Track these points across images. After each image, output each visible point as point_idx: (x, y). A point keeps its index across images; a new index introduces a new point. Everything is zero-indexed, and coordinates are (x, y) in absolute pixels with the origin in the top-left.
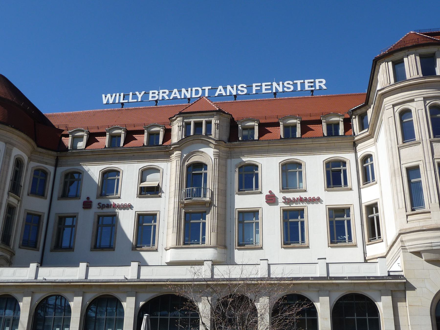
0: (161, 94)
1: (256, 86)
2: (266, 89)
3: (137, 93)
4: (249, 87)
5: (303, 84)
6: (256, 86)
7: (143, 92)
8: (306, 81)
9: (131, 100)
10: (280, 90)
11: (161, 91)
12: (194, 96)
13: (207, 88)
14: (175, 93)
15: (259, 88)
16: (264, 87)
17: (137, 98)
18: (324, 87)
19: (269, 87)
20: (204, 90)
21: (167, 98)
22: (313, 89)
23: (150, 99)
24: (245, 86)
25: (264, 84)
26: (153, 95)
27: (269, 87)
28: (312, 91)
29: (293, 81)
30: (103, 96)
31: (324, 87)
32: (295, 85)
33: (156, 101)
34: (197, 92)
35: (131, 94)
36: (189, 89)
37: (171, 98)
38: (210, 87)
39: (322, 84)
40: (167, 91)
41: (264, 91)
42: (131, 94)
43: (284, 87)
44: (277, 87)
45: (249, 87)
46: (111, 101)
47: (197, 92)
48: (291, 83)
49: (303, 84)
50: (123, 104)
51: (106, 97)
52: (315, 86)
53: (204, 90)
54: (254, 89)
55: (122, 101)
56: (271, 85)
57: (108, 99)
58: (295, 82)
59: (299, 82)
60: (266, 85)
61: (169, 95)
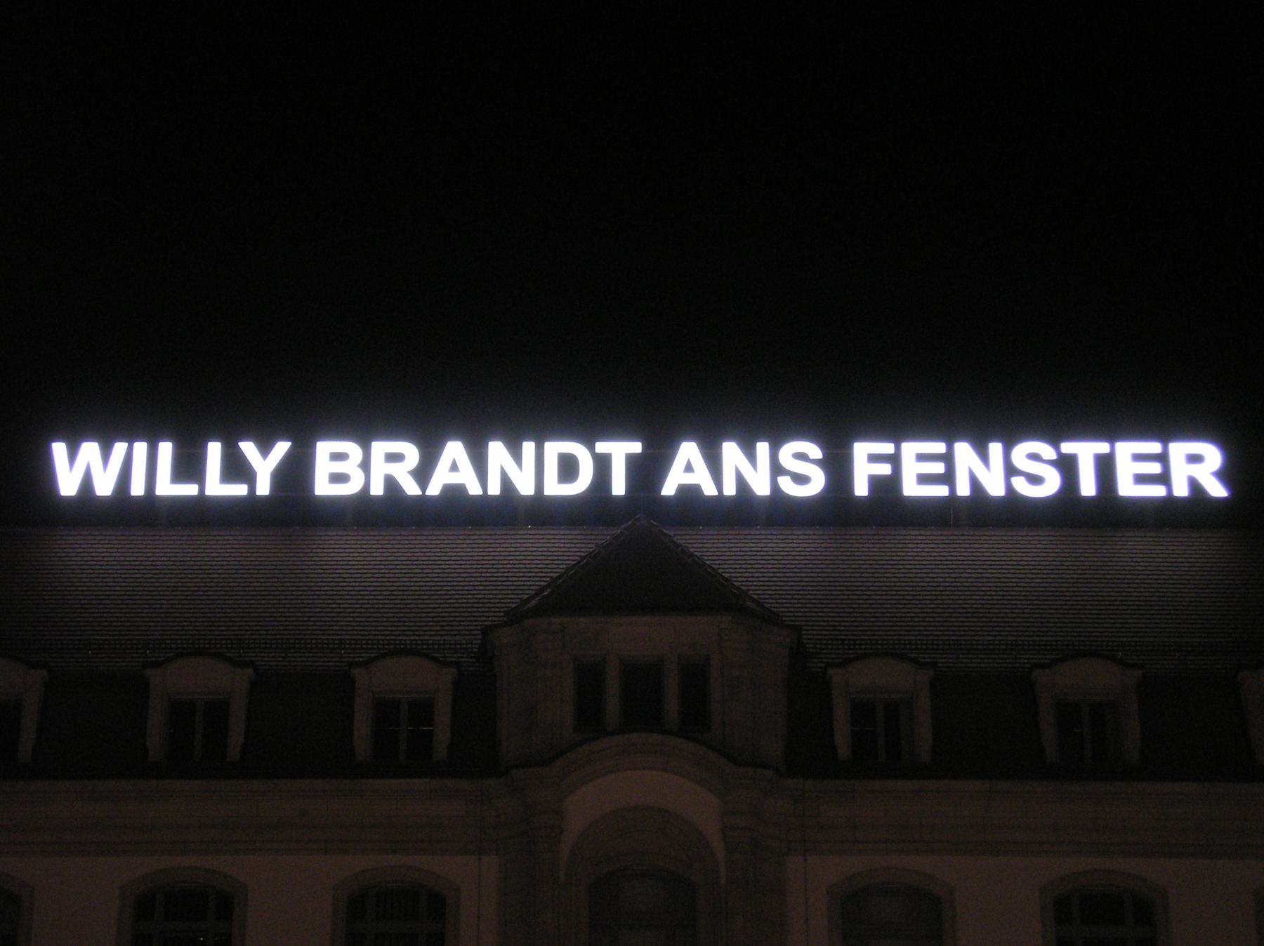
0: (380, 469)
1: (874, 458)
3: (248, 448)
4: (838, 467)
5: (1105, 467)
6: (874, 458)
7: (282, 448)
12: (554, 488)
14: (455, 467)
16: (911, 470)
18: (1217, 490)
20: (603, 464)
21: (411, 488)
25: (910, 449)
26: (339, 467)
27: (939, 468)
29: (1056, 445)
30: (59, 450)
31: (1217, 490)
32: (1067, 466)
34: (568, 468)
35: (214, 450)
37: (434, 489)
42: (214, 450)
43: (1011, 470)
45: (838, 467)
47: (568, 468)
48: (1047, 451)
49: (1105, 467)
53: (603, 464)
56: (948, 459)
57: (83, 468)
60: (922, 458)
61: (422, 474)
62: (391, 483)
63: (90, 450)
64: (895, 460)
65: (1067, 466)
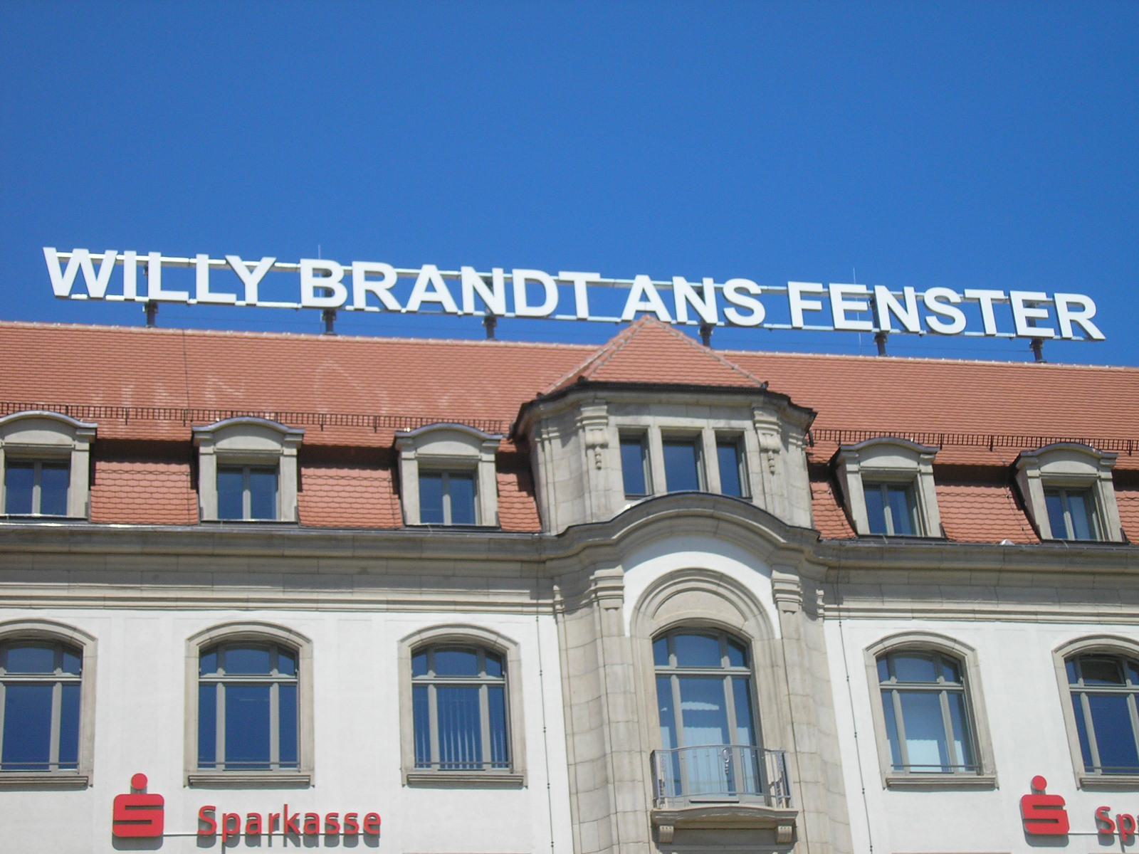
0: (360, 286)
1: (805, 295)
2: (849, 315)
5: (1004, 311)
6: (805, 295)
8: (1018, 297)
9: (204, 293)
10: (912, 321)
11: (359, 268)
12: (522, 308)
13: (581, 280)
15: (817, 305)
16: (839, 307)
17: (237, 286)
18: (1096, 333)
19: (1043, 313)
20: (566, 290)
21: (392, 303)
22: (1048, 332)
23: (308, 299)
24: (755, 288)
25: (836, 290)
28: (1037, 342)
29: (960, 291)
30: (52, 255)
31: (1096, 333)
32: (972, 310)
33: (330, 313)
34: (536, 293)
36: (498, 275)
37: (413, 305)
38: (595, 277)
39: (1083, 318)
40: (391, 274)
41: (840, 322)
44: (900, 307)
46: (97, 287)
47: (536, 293)
48: (954, 297)
49: (1004, 311)
50: (152, 306)
51: (64, 264)
52: (1053, 321)
53: (566, 290)
54: (797, 306)
55: (155, 292)
58: (970, 293)
59: (987, 297)
62: (372, 297)
63: (81, 257)
64: (826, 299)
65: (972, 310)
